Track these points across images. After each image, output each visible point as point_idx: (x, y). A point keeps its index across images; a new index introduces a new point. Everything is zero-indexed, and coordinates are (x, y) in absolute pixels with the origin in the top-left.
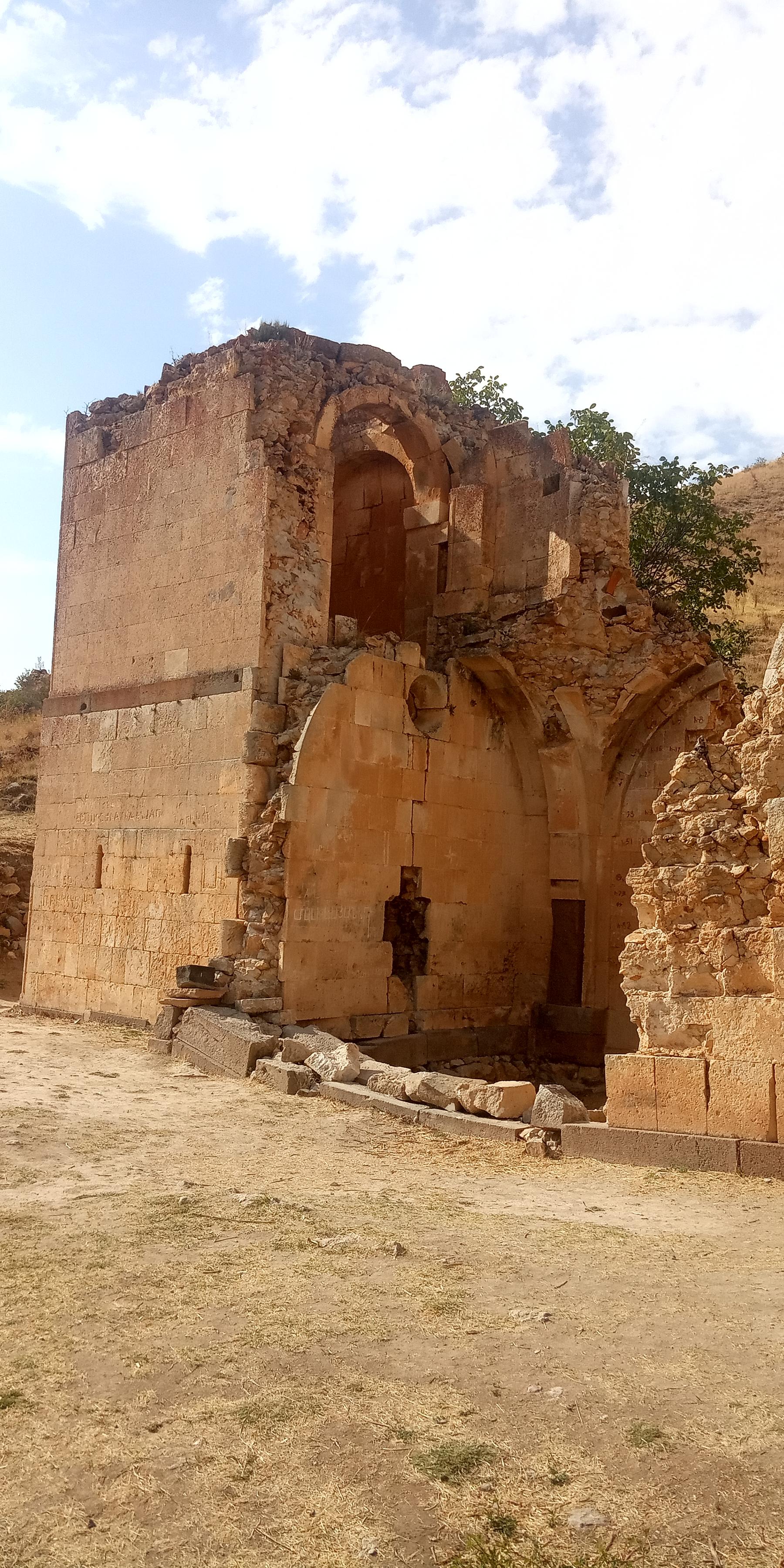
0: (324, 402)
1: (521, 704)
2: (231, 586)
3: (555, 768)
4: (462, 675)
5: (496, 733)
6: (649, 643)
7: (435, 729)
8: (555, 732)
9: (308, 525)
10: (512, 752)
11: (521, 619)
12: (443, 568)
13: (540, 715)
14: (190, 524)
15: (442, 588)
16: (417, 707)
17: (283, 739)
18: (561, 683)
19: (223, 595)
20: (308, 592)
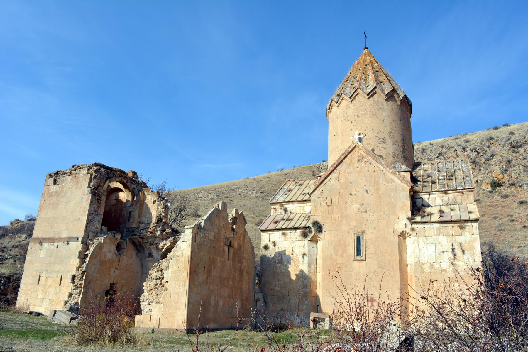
0: (106, 181)
1: (143, 249)
3: (149, 263)
4: (130, 241)
8: (150, 255)
9: (99, 207)
10: (141, 259)
12: (130, 216)
13: (147, 251)
16: (119, 247)
17: (86, 253)
18: (152, 245)
19: (77, 220)
20: (97, 221)
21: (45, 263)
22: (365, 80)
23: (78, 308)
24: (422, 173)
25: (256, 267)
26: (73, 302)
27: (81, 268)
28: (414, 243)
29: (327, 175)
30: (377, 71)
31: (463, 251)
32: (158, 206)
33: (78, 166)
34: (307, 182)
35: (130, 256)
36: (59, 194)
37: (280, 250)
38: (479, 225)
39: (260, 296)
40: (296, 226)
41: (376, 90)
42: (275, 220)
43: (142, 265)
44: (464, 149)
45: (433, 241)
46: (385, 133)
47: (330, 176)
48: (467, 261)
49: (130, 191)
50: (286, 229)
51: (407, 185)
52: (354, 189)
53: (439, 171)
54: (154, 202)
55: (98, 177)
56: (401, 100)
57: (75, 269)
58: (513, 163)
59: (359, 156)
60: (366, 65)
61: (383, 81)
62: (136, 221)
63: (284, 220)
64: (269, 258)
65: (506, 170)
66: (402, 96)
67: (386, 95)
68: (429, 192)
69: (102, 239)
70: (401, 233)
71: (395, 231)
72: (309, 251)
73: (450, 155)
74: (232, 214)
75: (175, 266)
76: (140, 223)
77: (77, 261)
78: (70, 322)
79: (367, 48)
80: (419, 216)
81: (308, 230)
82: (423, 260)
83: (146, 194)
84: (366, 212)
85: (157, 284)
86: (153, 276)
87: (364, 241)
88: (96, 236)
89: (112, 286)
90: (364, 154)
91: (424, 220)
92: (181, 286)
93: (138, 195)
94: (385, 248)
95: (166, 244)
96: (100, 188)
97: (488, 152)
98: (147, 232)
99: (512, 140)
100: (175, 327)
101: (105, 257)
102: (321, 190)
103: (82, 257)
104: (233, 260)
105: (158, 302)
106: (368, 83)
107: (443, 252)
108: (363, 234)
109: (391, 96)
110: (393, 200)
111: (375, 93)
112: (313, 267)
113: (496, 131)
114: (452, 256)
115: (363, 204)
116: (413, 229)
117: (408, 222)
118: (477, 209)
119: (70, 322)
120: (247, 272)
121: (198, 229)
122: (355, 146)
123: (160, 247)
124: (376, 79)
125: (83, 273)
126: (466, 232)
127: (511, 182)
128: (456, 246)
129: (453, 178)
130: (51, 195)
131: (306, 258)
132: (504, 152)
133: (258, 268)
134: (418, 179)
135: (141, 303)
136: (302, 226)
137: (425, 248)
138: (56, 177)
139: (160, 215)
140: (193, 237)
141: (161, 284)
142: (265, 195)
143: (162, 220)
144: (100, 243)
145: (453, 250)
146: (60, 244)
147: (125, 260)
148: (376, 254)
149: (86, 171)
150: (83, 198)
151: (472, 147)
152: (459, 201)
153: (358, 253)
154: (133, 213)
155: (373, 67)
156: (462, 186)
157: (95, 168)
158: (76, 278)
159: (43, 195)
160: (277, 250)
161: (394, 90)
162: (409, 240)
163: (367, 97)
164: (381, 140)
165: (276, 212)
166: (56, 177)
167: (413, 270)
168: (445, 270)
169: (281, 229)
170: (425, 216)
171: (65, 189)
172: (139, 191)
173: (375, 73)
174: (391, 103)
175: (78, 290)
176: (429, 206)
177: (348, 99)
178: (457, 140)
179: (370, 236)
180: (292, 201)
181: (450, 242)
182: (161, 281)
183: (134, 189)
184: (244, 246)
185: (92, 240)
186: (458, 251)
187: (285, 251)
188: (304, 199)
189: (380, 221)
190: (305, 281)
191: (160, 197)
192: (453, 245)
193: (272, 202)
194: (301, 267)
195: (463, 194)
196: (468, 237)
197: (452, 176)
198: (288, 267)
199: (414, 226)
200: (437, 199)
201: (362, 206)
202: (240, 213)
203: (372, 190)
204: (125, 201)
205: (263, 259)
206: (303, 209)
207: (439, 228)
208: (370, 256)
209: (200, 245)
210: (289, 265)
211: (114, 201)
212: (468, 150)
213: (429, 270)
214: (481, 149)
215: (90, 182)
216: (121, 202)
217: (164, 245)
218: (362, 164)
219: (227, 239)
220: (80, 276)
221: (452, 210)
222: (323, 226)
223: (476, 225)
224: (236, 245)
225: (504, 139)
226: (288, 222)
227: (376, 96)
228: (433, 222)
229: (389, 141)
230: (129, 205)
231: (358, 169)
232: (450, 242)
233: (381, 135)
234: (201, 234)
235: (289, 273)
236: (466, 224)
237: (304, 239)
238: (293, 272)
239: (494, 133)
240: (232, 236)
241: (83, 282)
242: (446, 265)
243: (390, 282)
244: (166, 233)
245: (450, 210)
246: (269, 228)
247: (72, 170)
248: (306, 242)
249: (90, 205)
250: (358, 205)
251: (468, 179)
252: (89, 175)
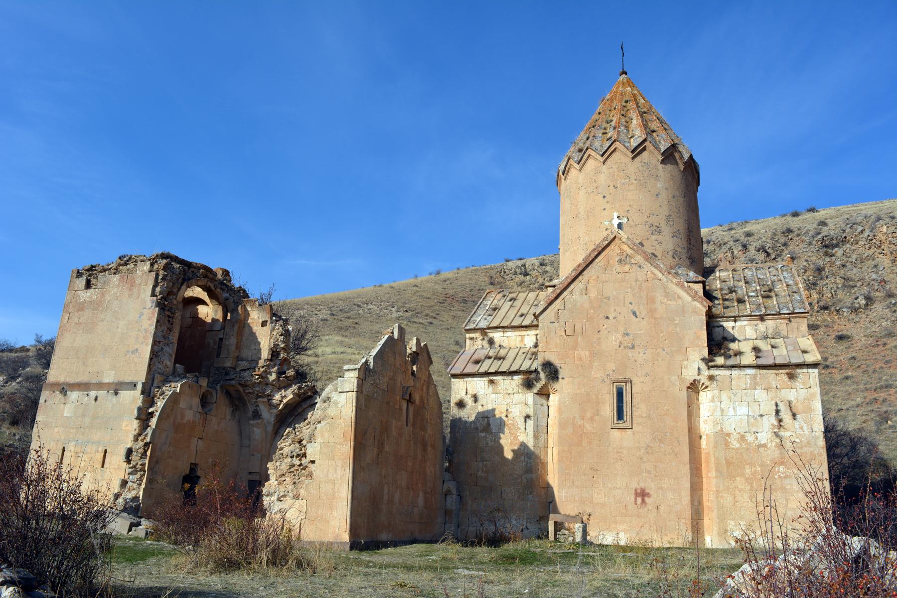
0: (182, 284)
1: (244, 404)
2: (137, 350)
4: (222, 391)
5: (233, 413)
7: (210, 410)
8: (257, 415)
9: (170, 330)
10: (239, 421)
12: (220, 347)
13: (251, 409)
14: (122, 323)
15: (218, 355)
16: (204, 401)
17: (150, 410)
18: (260, 397)
19: (133, 352)
21: (72, 428)
22: (627, 127)
23: (138, 507)
24: (718, 285)
25: (444, 438)
26: (129, 496)
27: (142, 437)
28: (713, 400)
29: (566, 284)
30: (645, 113)
31: (794, 415)
32: (273, 329)
33: (130, 258)
34: (522, 296)
35: (222, 418)
36: (96, 305)
37: (485, 408)
38: (820, 374)
39: (451, 485)
40: (512, 369)
41: (646, 144)
42: (476, 357)
43: (241, 433)
44: (745, 246)
45: (744, 398)
46: (660, 217)
47: (572, 286)
48: (799, 431)
49: (220, 304)
50: (496, 373)
51: (703, 305)
52: (612, 309)
53: (746, 282)
54: (264, 324)
55: (168, 278)
56: (685, 163)
57: (131, 437)
58: (826, 272)
59: (621, 254)
60: (626, 102)
61: (656, 129)
62: (231, 355)
63: (490, 358)
64: (466, 422)
65: (815, 284)
66: (686, 157)
67: (662, 154)
68: (735, 317)
69: (178, 386)
70: (691, 384)
71: (681, 380)
72: (535, 411)
73: (721, 255)
74: (412, 346)
75: (326, 435)
76: (238, 359)
77: (136, 424)
78: (130, 530)
79: (626, 73)
80: (720, 356)
81: (533, 376)
82: (728, 428)
83: (249, 309)
84: (633, 347)
85: (293, 466)
86: (286, 450)
87: (629, 395)
88: (166, 381)
89: (193, 468)
90: (629, 251)
91: (731, 362)
92: (339, 469)
93: (234, 311)
94: (665, 408)
95: (285, 396)
96: (171, 297)
97: (784, 254)
98: (252, 376)
99: (824, 234)
100: (329, 538)
101: (183, 417)
102: (556, 309)
103: (144, 417)
104: (414, 425)
105: (297, 497)
106: (631, 133)
107: (761, 416)
108: (629, 385)
109: (670, 155)
110: (678, 329)
111: (644, 149)
112: (542, 437)
113: (795, 219)
114: (776, 423)
116: (711, 378)
117: (703, 366)
118: (814, 347)
119: (130, 530)
120: (433, 446)
121: (365, 372)
122: (615, 237)
123: (274, 402)
124: (645, 125)
125: (147, 445)
126: (798, 384)
127: (821, 304)
128: (782, 407)
129: (772, 294)
130: (81, 307)
131: (530, 423)
132: (810, 254)
133: (448, 437)
134: (715, 294)
135: (264, 498)
136: (524, 368)
137: (731, 409)
138: (90, 275)
139: (276, 345)
140: (358, 384)
141: (301, 465)
142: (412, 316)
143: (278, 354)
144: (174, 393)
145: (777, 412)
146: (102, 394)
147: (214, 423)
148: (649, 417)
149: (147, 266)
150: (142, 314)
151: (758, 244)
152: (784, 333)
153: (620, 415)
154: (225, 342)
155: (638, 107)
156: (788, 309)
157: (164, 262)
158: (134, 454)
159: (66, 307)
160: (480, 409)
161: (674, 147)
162: (704, 397)
163: (631, 155)
164: (654, 228)
165: (475, 345)
166: (90, 275)
167: (712, 445)
168: (765, 446)
169: (487, 374)
170: (730, 356)
171: (108, 298)
172: (237, 304)
173: (641, 116)
174: (669, 167)
175: (138, 475)
176: (734, 340)
177: (599, 157)
178: (733, 232)
179: (639, 388)
180: (503, 327)
181: (772, 400)
182: (300, 460)
183: (227, 299)
184: (428, 400)
185: (159, 387)
186: (786, 415)
187: (494, 410)
188: (524, 324)
189: (656, 362)
190: (529, 461)
191: (274, 315)
192: (777, 405)
193: (467, 328)
194: (522, 438)
195: (790, 321)
196: (801, 391)
197: (770, 291)
198: (500, 438)
199: (714, 372)
200: (748, 329)
201: (627, 338)
202: (422, 345)
203: (642, 311)
204: (209, 320)
205: (456, 423)
206: (522, 340)
207: (755, 376)
208: (640, 420)
209: (368, 398)
210: (502, 435)
211: (189, 321)
212: (752, 249)
213: (738, 445)
214: (773, 248)
215: (155, 287)
216: (203, 322)
217: (282, 397)
218: (627, 268)
219: (406, 389)
220: (141, 450)
221: (773, 347)
222: (560, 370)
223: (814, 372)
224: (417, 398)
225: (811, 233)
226: (497, 363)
227: (645, 154)
228: (745, 367)
229: (667, 230)
230: (218, 327)
231: (620, 275)
232: (772, 400)
233: (654, 220)
234: (370, 380)
235: (501, 449)
236: (799, 371)
237: (527, 391)
238: (508, 445)
239: (794, 223)
240: (412, 384)
241: (147, 461)
242: (765, 436)
243: (674, 464)
244: (286, 377)
245: (770, 347)
246: (466, 371)
247: (120, 265)
248: (530, 397)
249: (156, 327)
250: (619, 336)
251: (797, 297)
252: (153, 274)
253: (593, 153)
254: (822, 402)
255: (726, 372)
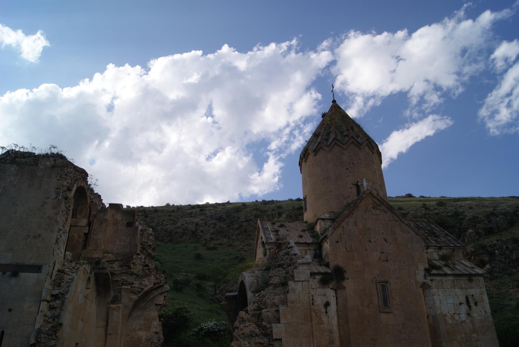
2: (40, 235)
6: (152, 276)
11: (116, 263)
13: (112, 294)
19: (35, 237)
70: (422, 284)
84: (387, 261)
115: (383, 253)
168: (464, 322)
213: (451, 322)
218: (378, 212)
223: (481, 279)
242: (463, 317)
253: (338, 143)
254: (488, 295)
255: (440, 278)
